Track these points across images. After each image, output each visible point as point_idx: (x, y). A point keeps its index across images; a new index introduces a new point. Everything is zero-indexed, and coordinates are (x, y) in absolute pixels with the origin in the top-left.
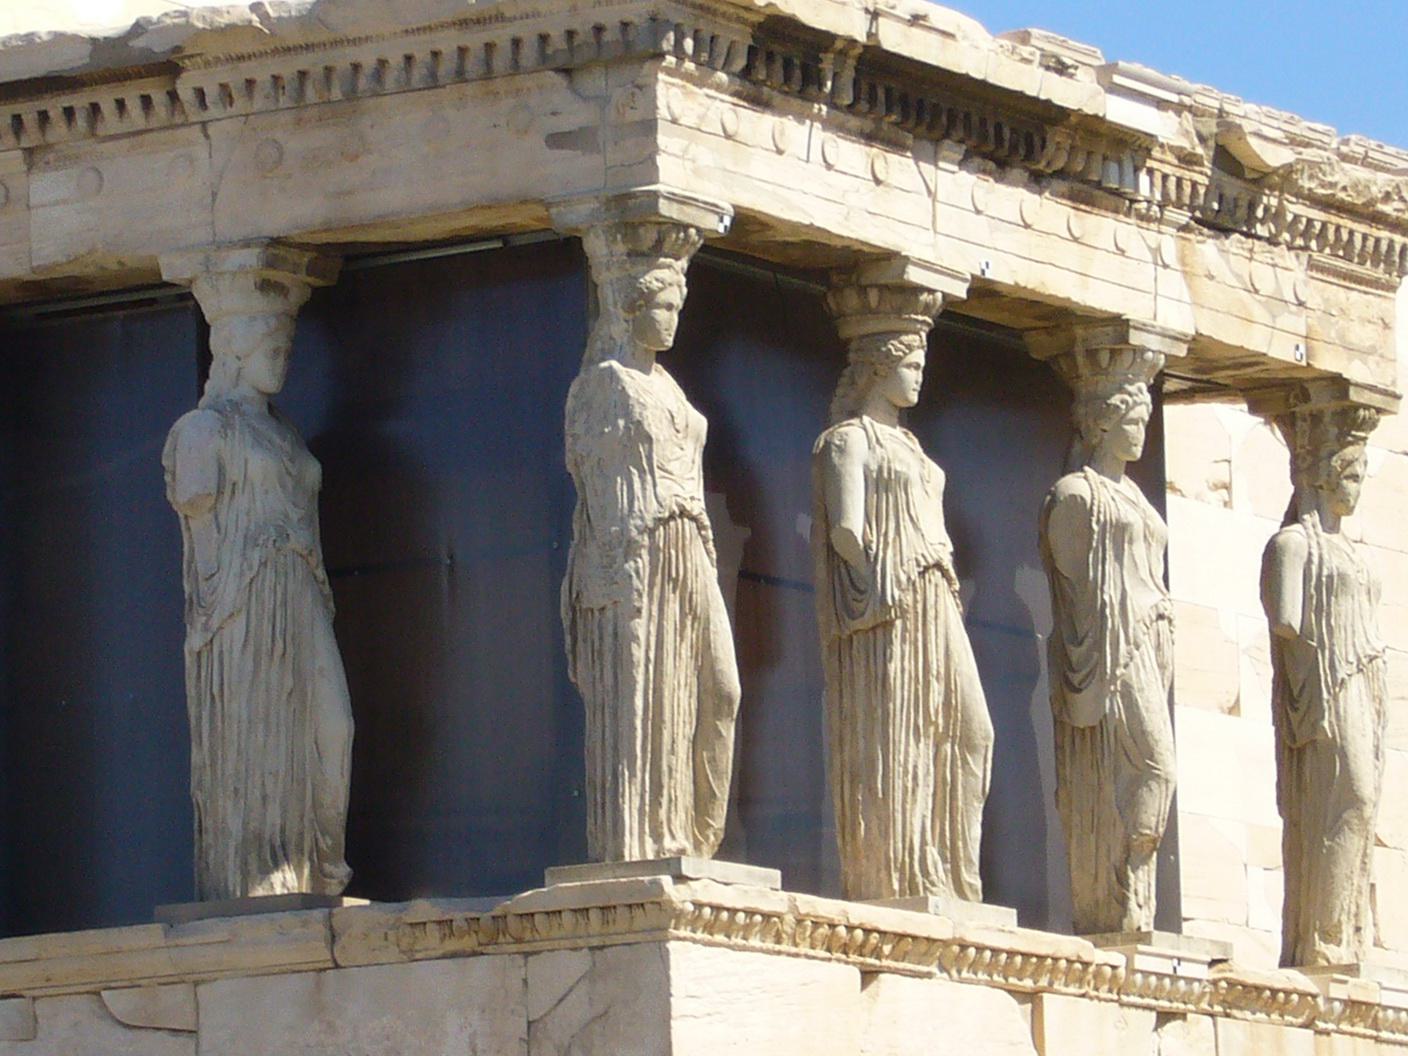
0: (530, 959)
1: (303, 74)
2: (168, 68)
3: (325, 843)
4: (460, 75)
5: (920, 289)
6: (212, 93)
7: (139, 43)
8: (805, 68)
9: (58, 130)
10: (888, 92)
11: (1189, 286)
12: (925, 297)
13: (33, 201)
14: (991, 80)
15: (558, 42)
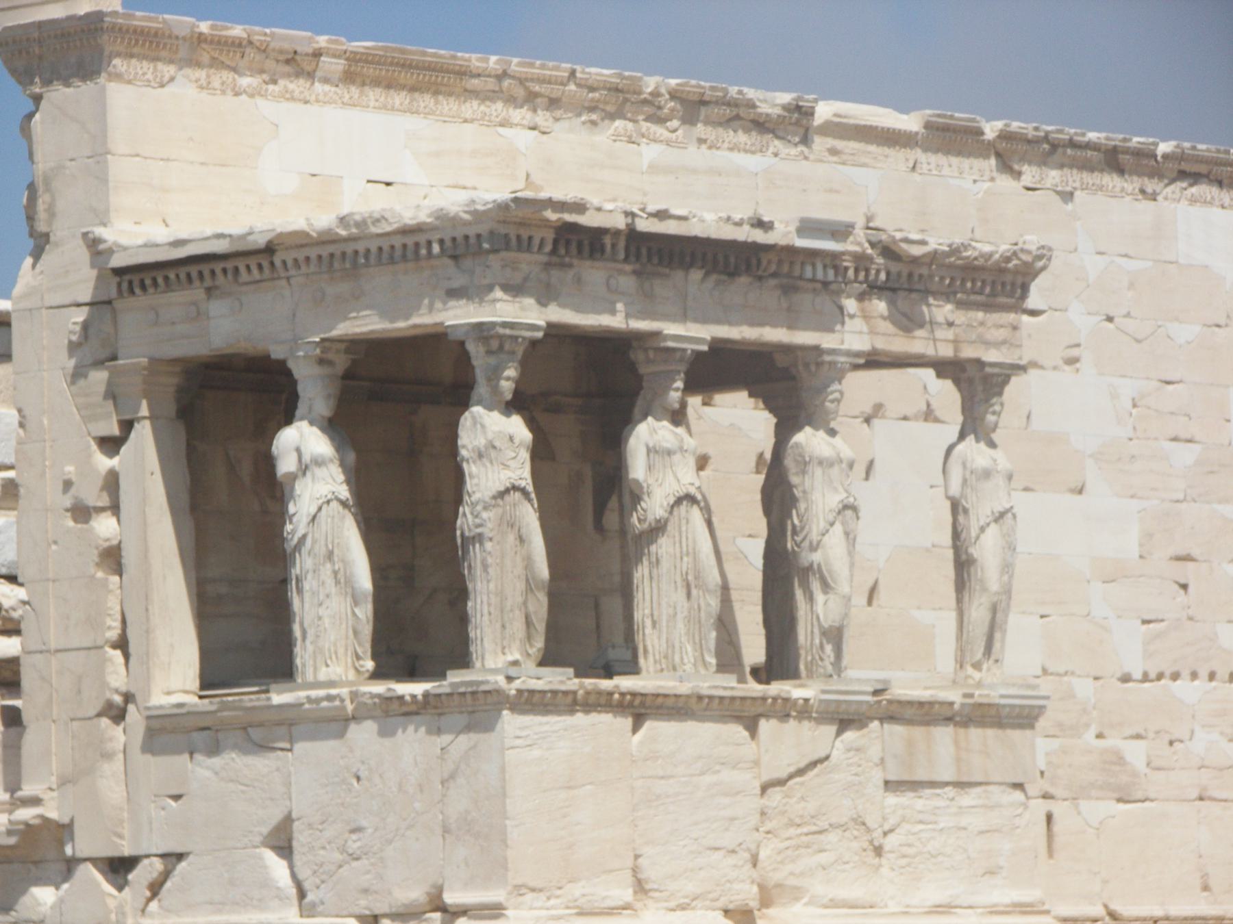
0: (443, 718)
1: (332, 255)
2: (269, 249)
3: (359, 651)
4: (404, 258)
5: (674, 350)
6: (290, 263)
7: (251, 238)
8: (592, 245)
9: (220, 278)
10: (649, 249)
11: (867, 323)
12: (678, 355)
13: (212, 314)
14: (714, 236)
15: (448, 243)
